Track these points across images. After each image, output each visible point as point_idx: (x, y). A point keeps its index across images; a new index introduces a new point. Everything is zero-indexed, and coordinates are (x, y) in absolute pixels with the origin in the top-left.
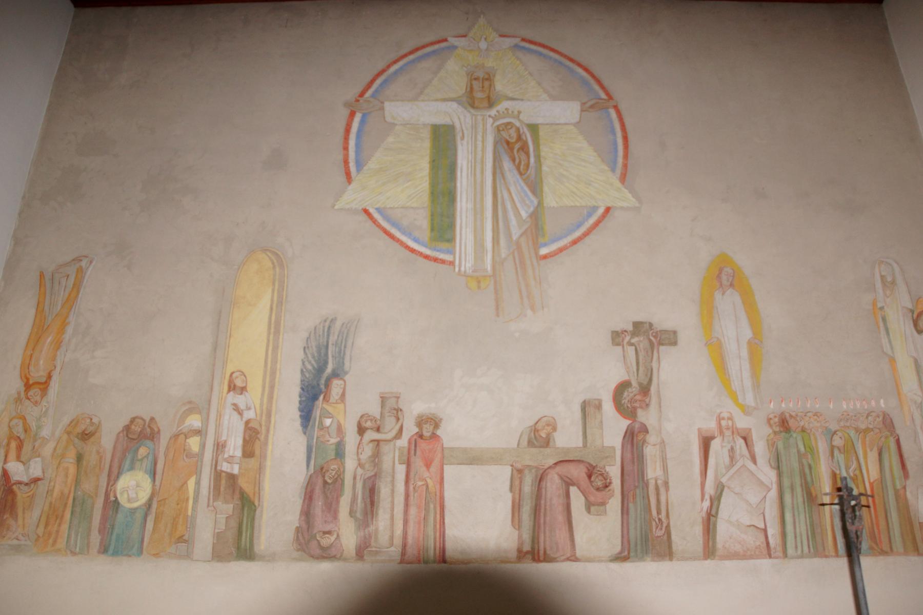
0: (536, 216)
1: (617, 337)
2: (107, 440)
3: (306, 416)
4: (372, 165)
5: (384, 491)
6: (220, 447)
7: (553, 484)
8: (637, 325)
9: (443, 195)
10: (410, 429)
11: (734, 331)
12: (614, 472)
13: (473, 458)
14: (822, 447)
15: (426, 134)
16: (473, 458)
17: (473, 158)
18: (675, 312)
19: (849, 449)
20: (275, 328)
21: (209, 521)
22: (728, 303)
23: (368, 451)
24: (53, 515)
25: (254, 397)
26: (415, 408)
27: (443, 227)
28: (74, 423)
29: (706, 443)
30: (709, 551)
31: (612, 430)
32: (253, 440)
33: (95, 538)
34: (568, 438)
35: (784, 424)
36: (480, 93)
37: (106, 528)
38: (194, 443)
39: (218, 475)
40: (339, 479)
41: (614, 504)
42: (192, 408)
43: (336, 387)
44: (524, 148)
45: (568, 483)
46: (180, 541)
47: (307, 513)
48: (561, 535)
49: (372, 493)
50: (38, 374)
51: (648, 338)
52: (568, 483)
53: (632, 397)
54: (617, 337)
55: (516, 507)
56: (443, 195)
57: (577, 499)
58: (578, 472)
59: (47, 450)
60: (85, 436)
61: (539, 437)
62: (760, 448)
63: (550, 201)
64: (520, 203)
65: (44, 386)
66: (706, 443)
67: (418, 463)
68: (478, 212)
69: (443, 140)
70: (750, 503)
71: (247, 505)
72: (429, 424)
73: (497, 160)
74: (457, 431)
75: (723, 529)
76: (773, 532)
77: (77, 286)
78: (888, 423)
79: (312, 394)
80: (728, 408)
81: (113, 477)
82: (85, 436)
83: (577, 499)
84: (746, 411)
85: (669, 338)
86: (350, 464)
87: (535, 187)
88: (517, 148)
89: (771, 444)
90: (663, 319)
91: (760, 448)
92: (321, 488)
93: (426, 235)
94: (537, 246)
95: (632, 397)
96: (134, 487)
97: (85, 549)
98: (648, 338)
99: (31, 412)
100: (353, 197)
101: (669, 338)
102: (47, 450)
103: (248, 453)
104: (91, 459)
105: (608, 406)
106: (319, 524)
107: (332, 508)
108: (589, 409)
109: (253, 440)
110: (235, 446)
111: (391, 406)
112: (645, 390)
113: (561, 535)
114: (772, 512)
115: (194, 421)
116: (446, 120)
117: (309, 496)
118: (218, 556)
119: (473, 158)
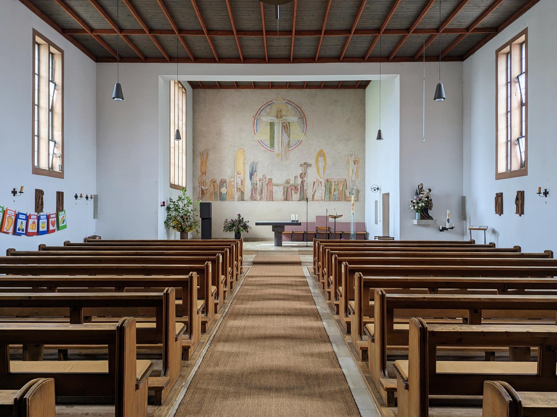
0: (289, 142)
1: (301, 165)
2: (218, 182)
3: (251, 178)
4: (259, 131)
5: (264, 190)
6: (237, 184)
7: (289, 189)
8: (305, 164)
9: (272, 138)
10: (267, 181)
11: (321, 164)
12: (299, 188)
13: (277, 185)
14: (333, 184)
15: (269, 124)
16: (277, 185)
17: (278, 129)
18: (312, 161)
19: (338, 184)
20: (244, 163)
21: (237, 195)
22: (321, 159)
23: (261, 184)
24: (211, 195)
25: (241, 176)
26: (269, 177)
27: (272, 145)
28: (212, 180)
29: (314, 183)
30: (313, 200)
31: (299, 181)
32: (242, 182)
33: (219, 198)
34: (292, 182)
35: (328, 181)
36: (279, 115)
37: (220, 196)
38: (233, 183)
39: (237, 188)
40: (257, 188)
41: (299, 192)
42: (232, 177)
43: (255, 174)
44: (287, 128)
45: (292, 189)
46: (233, 199)
47: (252, 194)
48: (290, 197)
49: (262, 190)
50: (203, 171)
51: (306, 165)
52: (292, 189)
53: (303, 175)
54: (301, 165)
55: (284, 193)
56: (272, 138)
57: (293, 192)
58: (293, 188)
59: (208, 184)
60: (214, 182)
61: (288, 182)
62: (323, 184)
63: (291, 139)
64: (286, 140)
65: (205, 173)
66: (314, 183)
67: (269, 186)
68: (278, 145)
69: (272, 125)
70: (321, 192)
71: (242, 193)
72: (270, 180)
73: (282, 130)
74: (275, 181)
75: (315, 196)
76: (323, 197)
77: (207, 155)
78: (345, 180)
79: (251, 175)
80: (319, 178)
81: (220, 188)
82: (214, 182)
83: (293, 192)
84: (321, 178)
85: (310, 165)
86: (258, 186)
87: (289, 136)
88: (286, 127)
89: (325, 184)
90: (309, 161)
91: (323, 184)
92: (254, 190)
93: (269, 146)
94: (289, 148)
95: (303, 175)
96: (224, 190)
97: (217, 200)
98: (306, 165)
99: (204, 178)
100: (257, 138)
101: (310, 165)
102: (208, 184)
103: (242, 185)
104: (216, 186)
105: (299, 177)
106: (254, 196)
107: (256, 193)
108: (296, 177)
109: (242, 182)
110: (240, 183)
111: (264, 176)
112: (305, 174)
113: (290, 197)
114: (323, 194)
115: (232, 180)
116: (272, 121)
117: (252, 191)
118: (238, 200)
119: (278, 129)
